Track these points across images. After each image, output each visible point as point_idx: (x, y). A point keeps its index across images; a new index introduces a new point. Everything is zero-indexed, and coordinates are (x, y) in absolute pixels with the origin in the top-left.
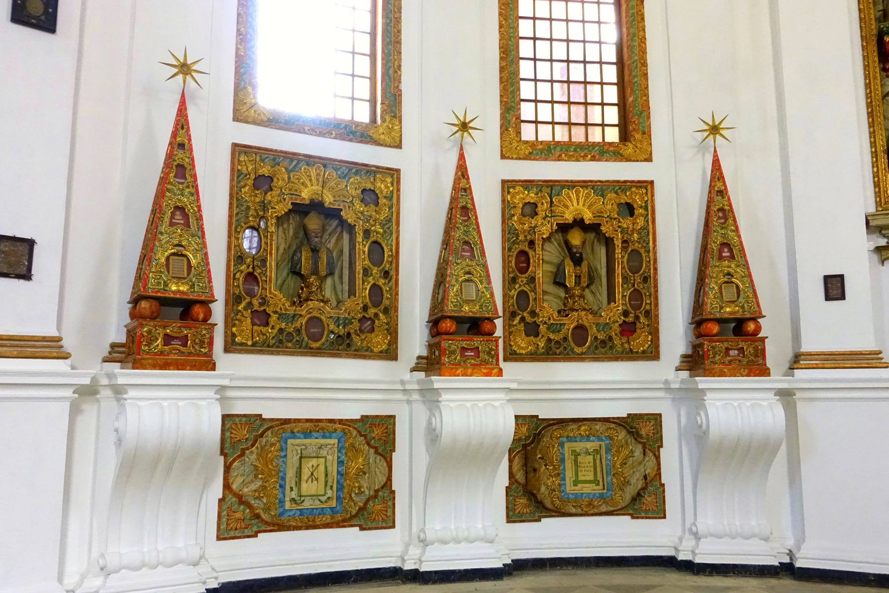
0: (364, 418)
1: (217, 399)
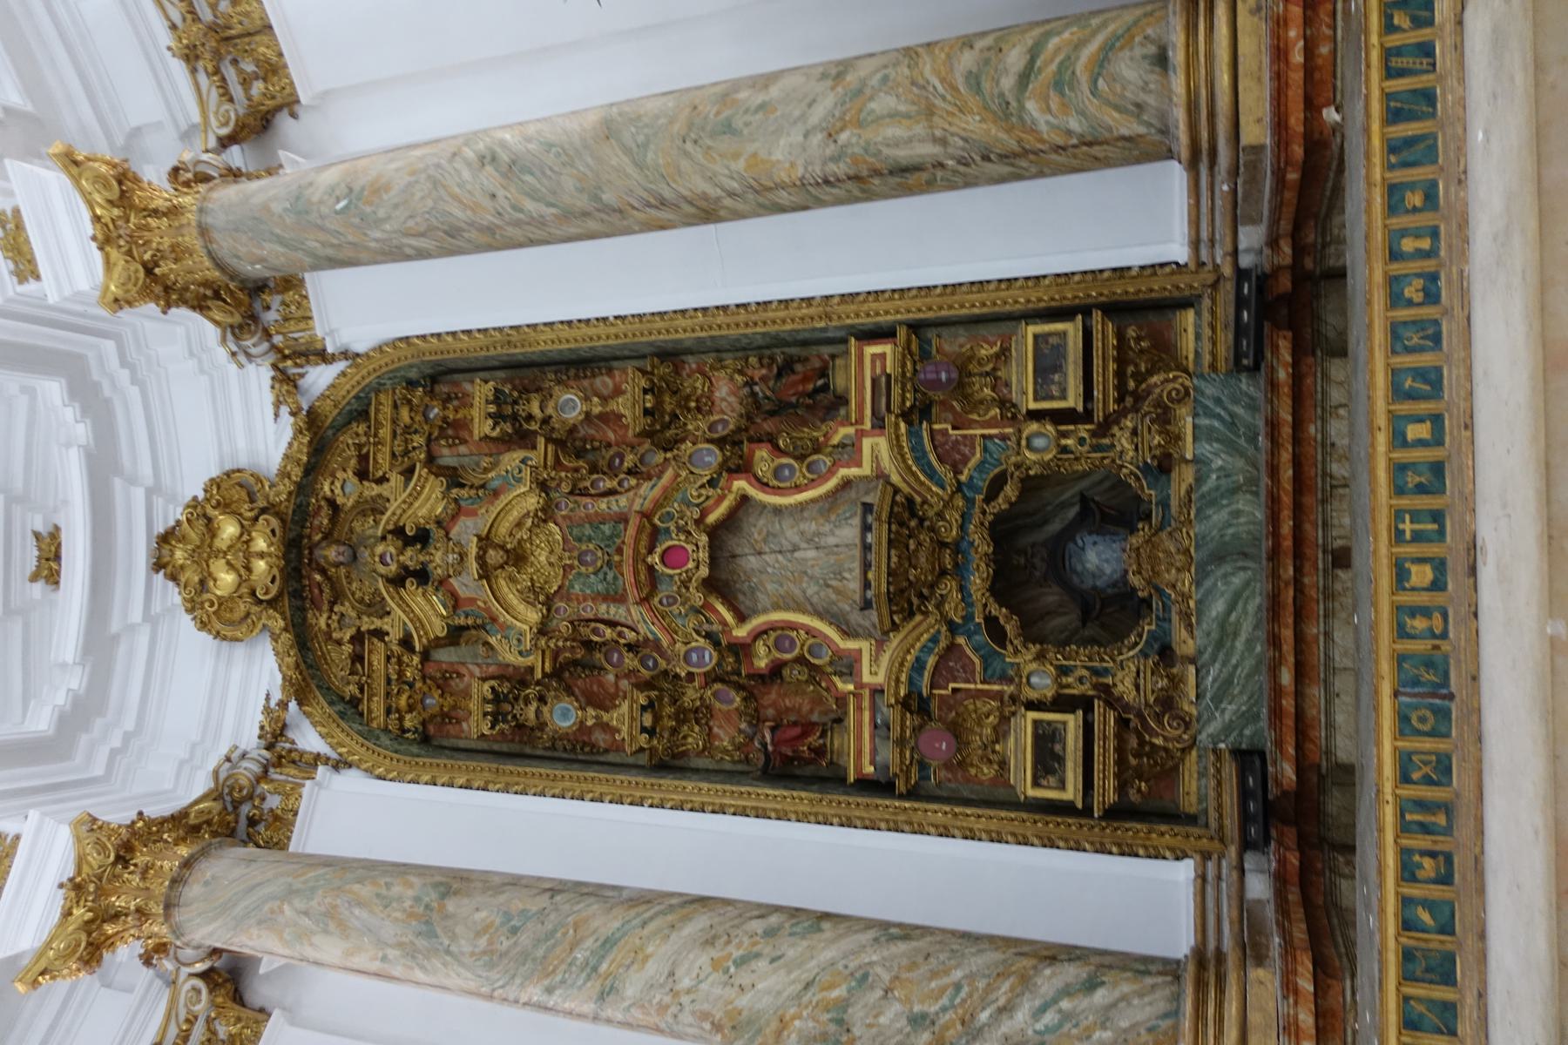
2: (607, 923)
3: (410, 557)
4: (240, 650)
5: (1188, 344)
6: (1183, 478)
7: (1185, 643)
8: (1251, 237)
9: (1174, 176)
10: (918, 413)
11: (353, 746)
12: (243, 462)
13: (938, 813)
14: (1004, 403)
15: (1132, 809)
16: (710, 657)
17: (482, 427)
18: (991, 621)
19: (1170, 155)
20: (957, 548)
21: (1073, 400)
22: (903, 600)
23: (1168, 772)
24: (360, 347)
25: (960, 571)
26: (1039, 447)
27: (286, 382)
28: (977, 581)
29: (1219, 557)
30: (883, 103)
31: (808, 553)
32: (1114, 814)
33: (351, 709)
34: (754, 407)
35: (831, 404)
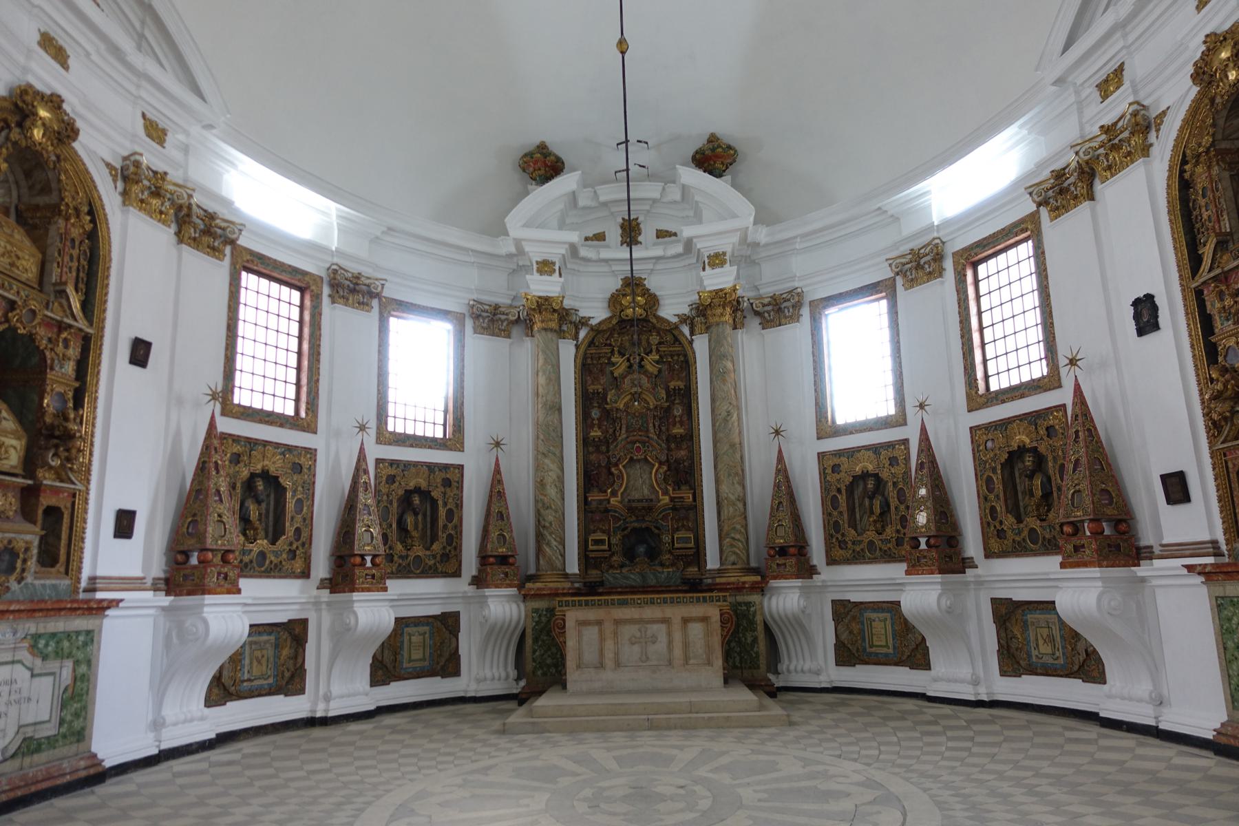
0: (290, 621)
1: (163, 609)
2: (557, 453)
3: (636, 367)
4: (606, 305)
5: (691, 569)
6: (660, 569)
7: (625, 570)
8: (709, 581)
9: (717, 566)
10: (674, 509)
11: (583, 348)
12: (661, 302)
13: (582, 516)
14: (678, 529)
15: (586, 559)
16: (614, 460)
17: (672, 385)
18: (626, 528)
19: (722, 564)
20: (643, 520)
21: (676, 545)
22: (631, 510)
23: (597, 566)
24: (695, 345)
25: (637, 521)
26: (666, 538)
27: (684, 319)
28: (636, 525)
29: (643, 577)
30: (731, 509)
31: (642, 482)
32: (586, 557)
33: (591, 344)
34: (677, 462)
35: (678, 485)
